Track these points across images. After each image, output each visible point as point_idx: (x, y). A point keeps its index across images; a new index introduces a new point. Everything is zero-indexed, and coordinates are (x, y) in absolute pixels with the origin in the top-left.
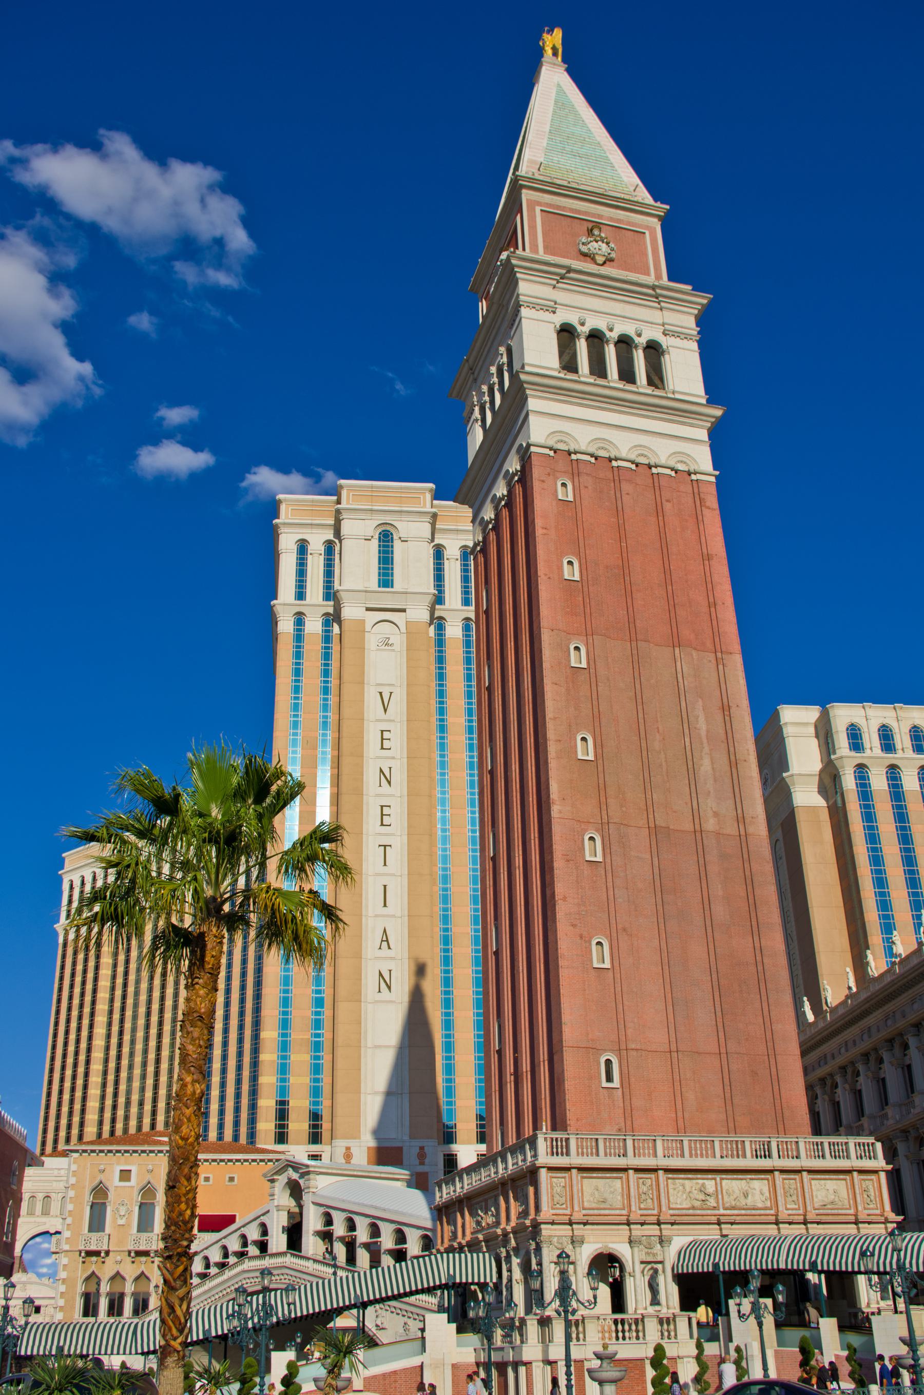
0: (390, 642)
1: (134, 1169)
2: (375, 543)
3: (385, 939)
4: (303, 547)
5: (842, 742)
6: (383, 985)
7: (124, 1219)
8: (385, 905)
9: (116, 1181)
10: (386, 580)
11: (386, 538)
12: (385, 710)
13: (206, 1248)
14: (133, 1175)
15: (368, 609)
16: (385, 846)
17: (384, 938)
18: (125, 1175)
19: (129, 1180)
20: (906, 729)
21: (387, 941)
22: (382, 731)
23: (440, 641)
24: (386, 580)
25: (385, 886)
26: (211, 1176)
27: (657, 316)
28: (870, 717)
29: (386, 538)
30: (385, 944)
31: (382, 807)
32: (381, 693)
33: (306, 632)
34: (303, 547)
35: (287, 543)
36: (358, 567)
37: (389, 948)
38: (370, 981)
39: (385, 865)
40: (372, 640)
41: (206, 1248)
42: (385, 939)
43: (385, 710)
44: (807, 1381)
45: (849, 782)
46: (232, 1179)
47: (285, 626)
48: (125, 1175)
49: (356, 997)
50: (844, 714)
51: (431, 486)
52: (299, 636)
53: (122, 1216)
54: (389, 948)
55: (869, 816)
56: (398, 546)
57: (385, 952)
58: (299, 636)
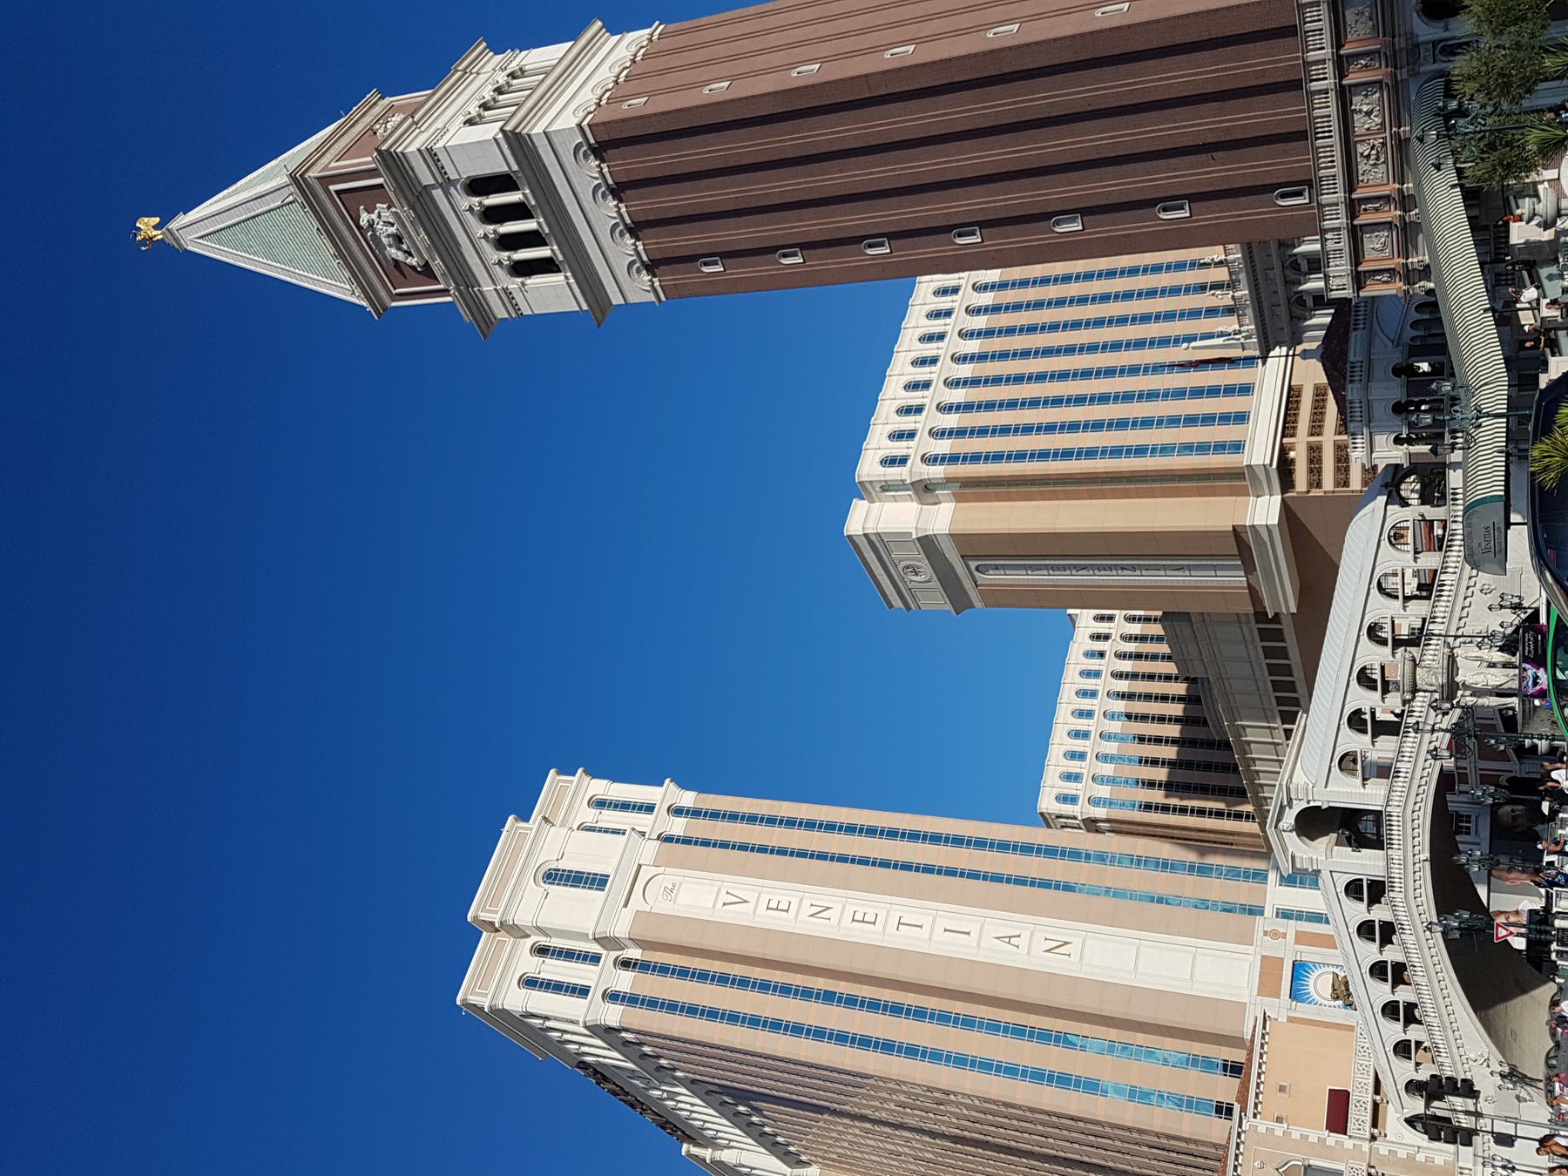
2: (553, 888)
4: (530, 983)
5: (895, 473)
10: (599, 882)
11: (554, 877)
15: (626, 905)
20: (898, 419)
23: (687, 841)
24: (599, 882)
27: (482, 78)
28: (877, 444)
29: (554, 877)
34: (530, 983)
35: (517, 1000)
36: (574, 913)
40: (662, 906)
45: (938, 472)
46: (1282, 1089)
47: (613, 1015)
50: (869, 467)
51: (511, 818)
52: (632, 1000)
55: (976, 458)
56: (564, 865)
57: (1022, 942)
58: (632, 1000)
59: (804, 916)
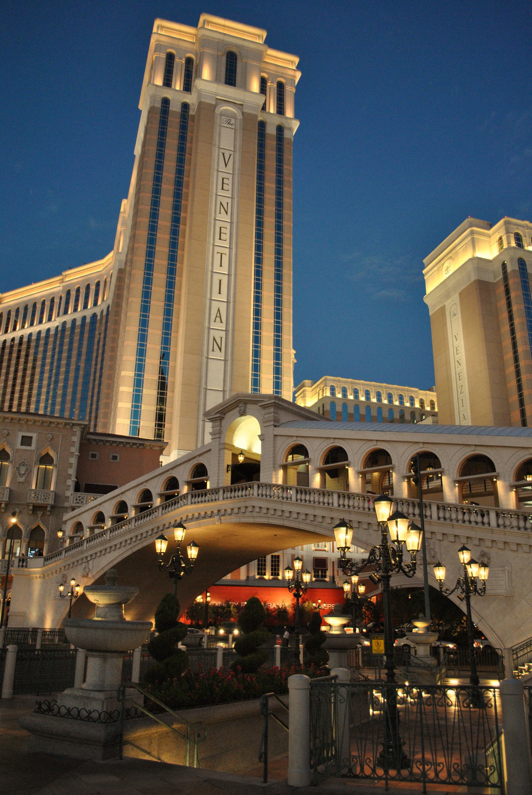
0: (231, 122)
1: (34, 436)
2: (224, 59)
6: (216, 347)
7: (24, 478)
8: (220, 293)
9: (19, 446)
12: (226, 165)
13: (200, 455)
14: (34, 441)
16: (222, 254)
17: (218, 315)
18: (27, 441)
19: (30, 445)
22: (223, 179)
26: (90, 459)
30: (218, 319)
32: (223, 154)
33: (171, 108)
37: (221, 322)
39: (221, 266)
41: (200, 455)
43: (226, 165)
44: (439, 631)
46: (115, 458)
48: (27, 441)
53: (21, 475)
54: (221, 322)
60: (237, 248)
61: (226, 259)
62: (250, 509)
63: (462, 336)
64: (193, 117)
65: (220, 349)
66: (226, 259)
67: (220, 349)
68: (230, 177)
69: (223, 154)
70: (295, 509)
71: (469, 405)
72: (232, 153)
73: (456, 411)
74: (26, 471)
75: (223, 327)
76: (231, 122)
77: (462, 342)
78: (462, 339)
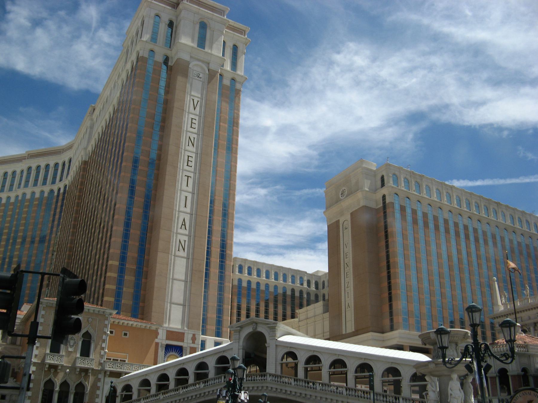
0: (200, 76)
3: (184, 224)
6: (181, 247)
12: (195, 109)
16: (188, 177)
21: (185, 225)
25: (186, 197)
30: (183, 226)
31: (188, 156)
32: (193, 100)
38: (174, 245)
42: (184, 224)
43: (195, 109)
46: (126, 334)
49: (167, 251)
59: (189, 134)
60: (200, 173)
61: (191, 181)
62: (265, 388)
63: (351, 245)
64: (171, 66)
65: (184, 250)
66: (191, 181)
67: (184, 250)
68: (197, 118)
69: (193, 100)
70: (294, 390)
71: (352, 297)
72: (199, 100)
73: (343, 300)
74: (74, 344)
75: (187, 232)
76: (200, 76)
77: (351, 249)
78: (351, 248)
